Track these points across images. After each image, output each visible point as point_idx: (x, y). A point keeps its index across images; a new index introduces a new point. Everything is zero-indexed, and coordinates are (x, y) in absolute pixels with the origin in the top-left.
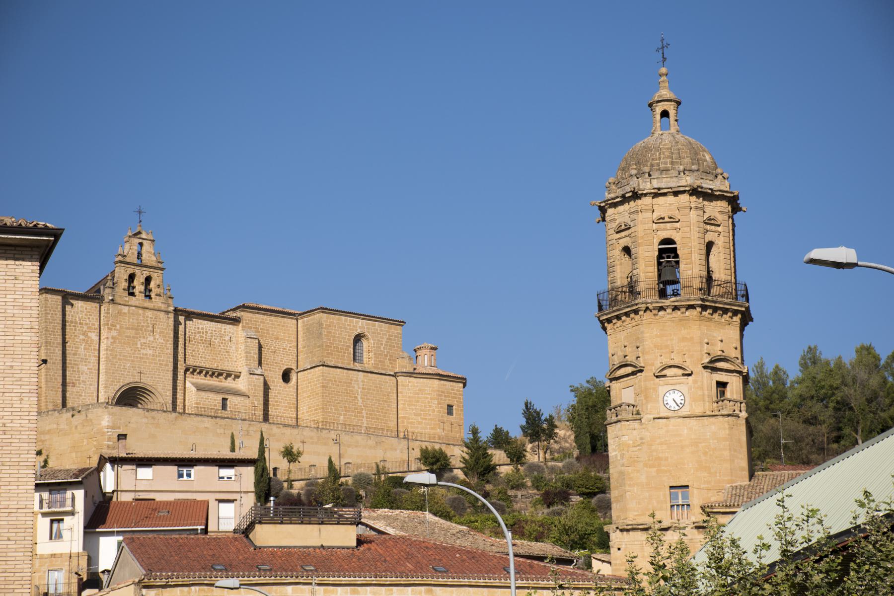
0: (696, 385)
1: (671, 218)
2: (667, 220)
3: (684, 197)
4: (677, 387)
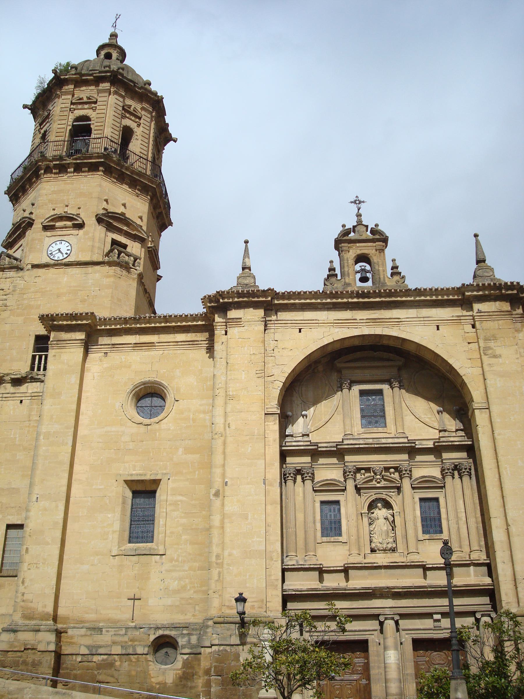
0: (87, 237)
2: (85, 100)
3: (106, 85)
4: (65, 238)
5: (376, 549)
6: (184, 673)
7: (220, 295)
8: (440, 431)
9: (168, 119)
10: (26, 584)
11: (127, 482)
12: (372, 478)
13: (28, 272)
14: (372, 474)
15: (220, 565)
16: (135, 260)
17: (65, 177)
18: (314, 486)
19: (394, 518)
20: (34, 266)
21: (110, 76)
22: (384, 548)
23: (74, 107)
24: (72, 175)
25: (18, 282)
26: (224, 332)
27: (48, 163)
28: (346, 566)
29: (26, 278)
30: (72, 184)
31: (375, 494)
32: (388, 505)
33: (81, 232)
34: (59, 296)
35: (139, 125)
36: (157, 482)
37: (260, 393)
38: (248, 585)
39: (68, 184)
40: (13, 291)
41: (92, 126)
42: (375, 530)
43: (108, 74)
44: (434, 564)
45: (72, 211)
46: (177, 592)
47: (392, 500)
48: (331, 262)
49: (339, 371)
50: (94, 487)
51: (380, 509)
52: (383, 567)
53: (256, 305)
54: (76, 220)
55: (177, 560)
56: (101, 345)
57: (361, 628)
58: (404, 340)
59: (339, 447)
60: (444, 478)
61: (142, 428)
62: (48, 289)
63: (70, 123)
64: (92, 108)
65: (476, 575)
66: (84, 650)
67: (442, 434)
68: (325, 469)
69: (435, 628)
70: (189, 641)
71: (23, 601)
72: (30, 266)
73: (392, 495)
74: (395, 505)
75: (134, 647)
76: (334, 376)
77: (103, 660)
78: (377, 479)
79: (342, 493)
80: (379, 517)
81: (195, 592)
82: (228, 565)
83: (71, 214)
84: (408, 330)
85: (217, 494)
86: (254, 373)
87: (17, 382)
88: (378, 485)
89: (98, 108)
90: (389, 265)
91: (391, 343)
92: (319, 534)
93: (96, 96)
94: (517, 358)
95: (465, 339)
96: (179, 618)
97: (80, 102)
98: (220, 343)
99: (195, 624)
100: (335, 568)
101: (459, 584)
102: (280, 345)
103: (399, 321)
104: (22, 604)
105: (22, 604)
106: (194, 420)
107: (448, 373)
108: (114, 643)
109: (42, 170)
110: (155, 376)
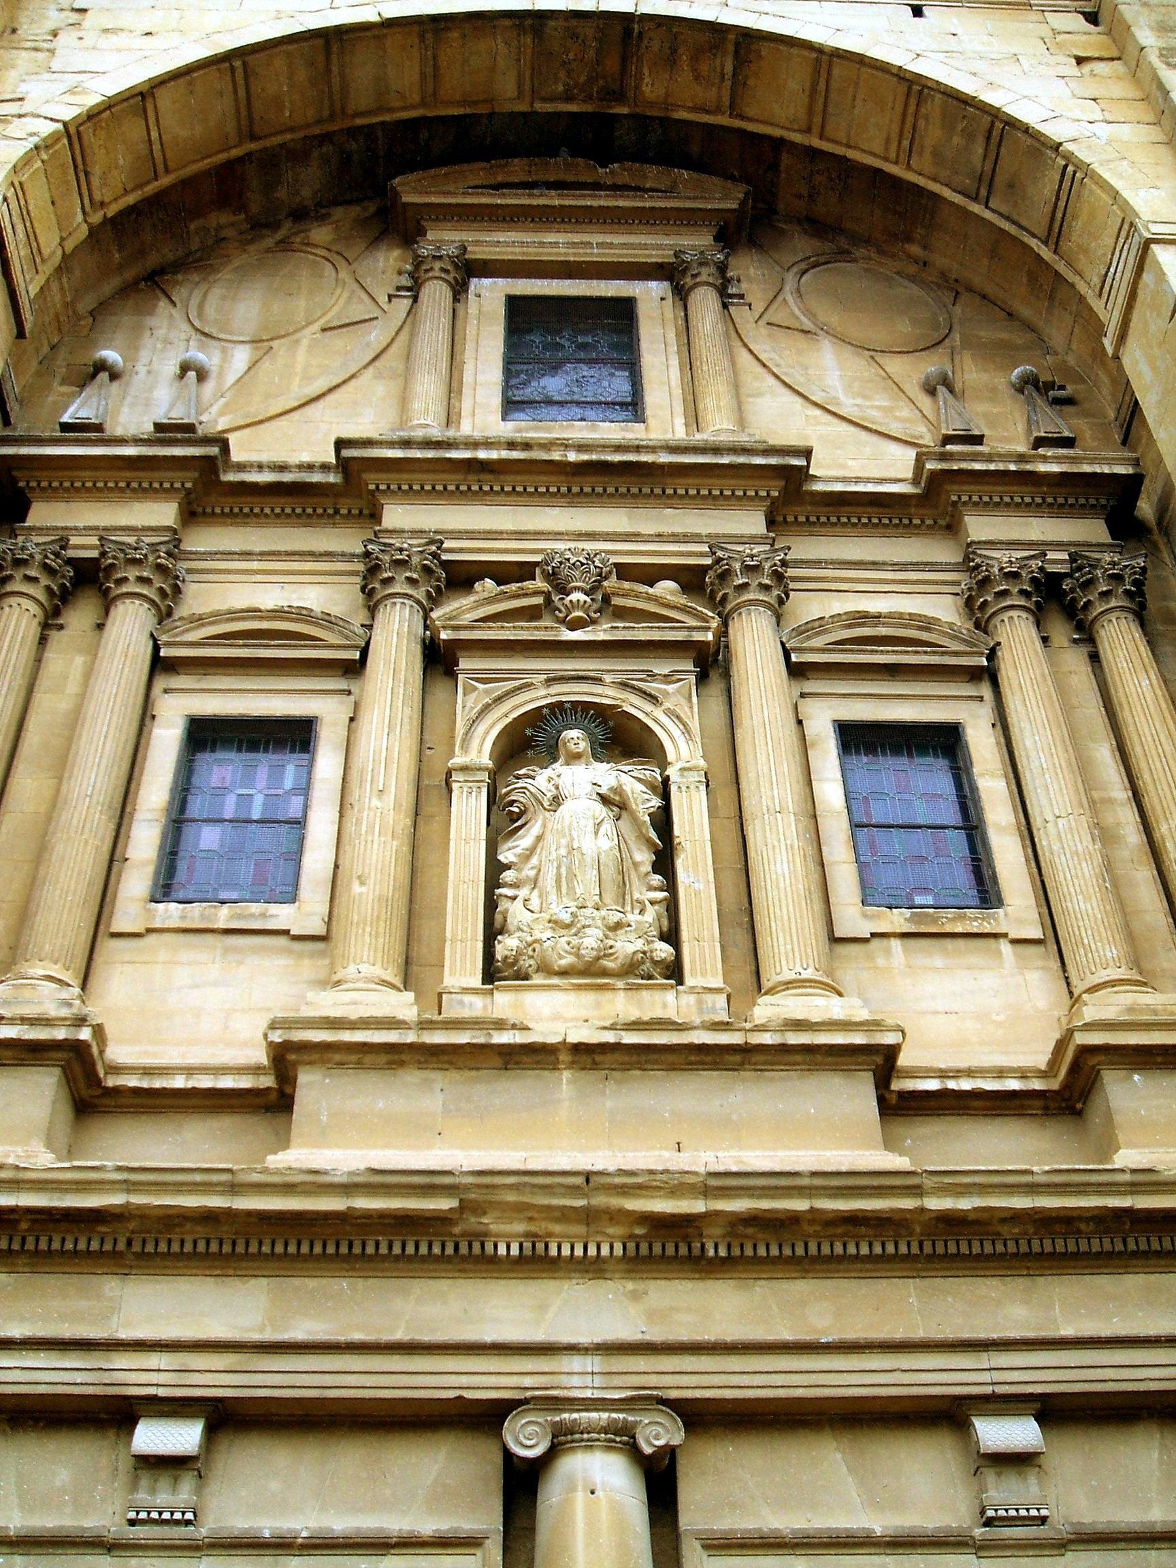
5: (526, 963)
12: (539, 600)
14: (540, 584)
18: (164, 638)
19: (666, 796)
22: (589, 955)
28: (277, 1037)
31: (550, 681)
42: (534, 861)
44: (958, 1073)
47: (659, 713)
51: (574, 757)
52: (564, 1057)
57: (340, 1524)
59: (346, 453)
60: (982, 626)
68: (259, 578)
73: (666, 693)
74: (681, 740)
78: (576, 605)
79: (342, 684)
80: (565, 791)
100: (205, 1082)
107: (975, 199)
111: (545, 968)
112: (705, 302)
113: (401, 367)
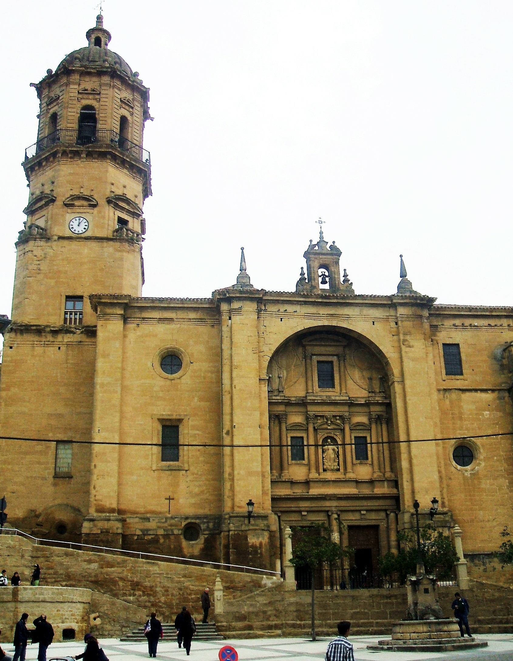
0: (100, 215)
1: (94, 91)
3: (106, 79)
4: (82, 215)
6: (205, 546)
7: (227, 292)
8: (369, 392)
9: (149, 104)
10: (97, 489)
11: (161, 420)
13: (55, 243)
15: (233, 480)
16: (138, 235)
17: (79, 162)
20: (61, 238)
21: (111, 72)
23: (80, 96)
24: (85, 160)
25: (48, 250)
26: (228, 318)
27: (65, 149)
29: (55, 248)
30: (85, 168)
32: (334, 442)
33: (96, 210)
34: (82, 264)
35: (132, 114)
36: (180, 421)
37: (255, 365)
38: (250, 493)
39: (82, 167)
40: (45, 258)
41: (97, 116)
43: (109, 70)
45: (86, 193)
46: (197, 495)
48: (302, 268)
49: (304, 346)
50: (137, 423)
53: (252, 299)
54: (90, 201)
55: (197, 474)
56: (134, 318)
58: (351, 330)
60: (370, 424)
61: (168, 382)
62: (73, 258)
63: (79, 112)
64: (96, 99)
65: (388, 487)
66: (139, 533)
67: (370, 395)
69: (361, 519)
70: (208, 527)
71: (96, 500)
72: (56, 238)
75: (172, 530)
76: (300, 350)
77: (152, 538)
81: (209, 495)
82: (238, 480)
83: (87, 195)
84: (354, 324)
85: (228, 433)
86: (252, 349)
87: (55, 333)
88: (329, 428)
89: (102, 99)
90: (342, 273)
91: (341, 331)
92: (290, 459)
93: (98, 88)
94: (424, 349)
95: (390, 332)
96: (201, 512)
97: (84, 92)
98: (226, 326)
99: (211, 515)
101: (378, 493)
102: (268, 329)
103: (348, 317)
104: (95, 502)
105: (95, 502)
106: (205, 378)
108: (159, 527)
109: (59, 153)
110: (174, 343)
111: (329, 470)
112: (342, 362)
113: (305, 375)
